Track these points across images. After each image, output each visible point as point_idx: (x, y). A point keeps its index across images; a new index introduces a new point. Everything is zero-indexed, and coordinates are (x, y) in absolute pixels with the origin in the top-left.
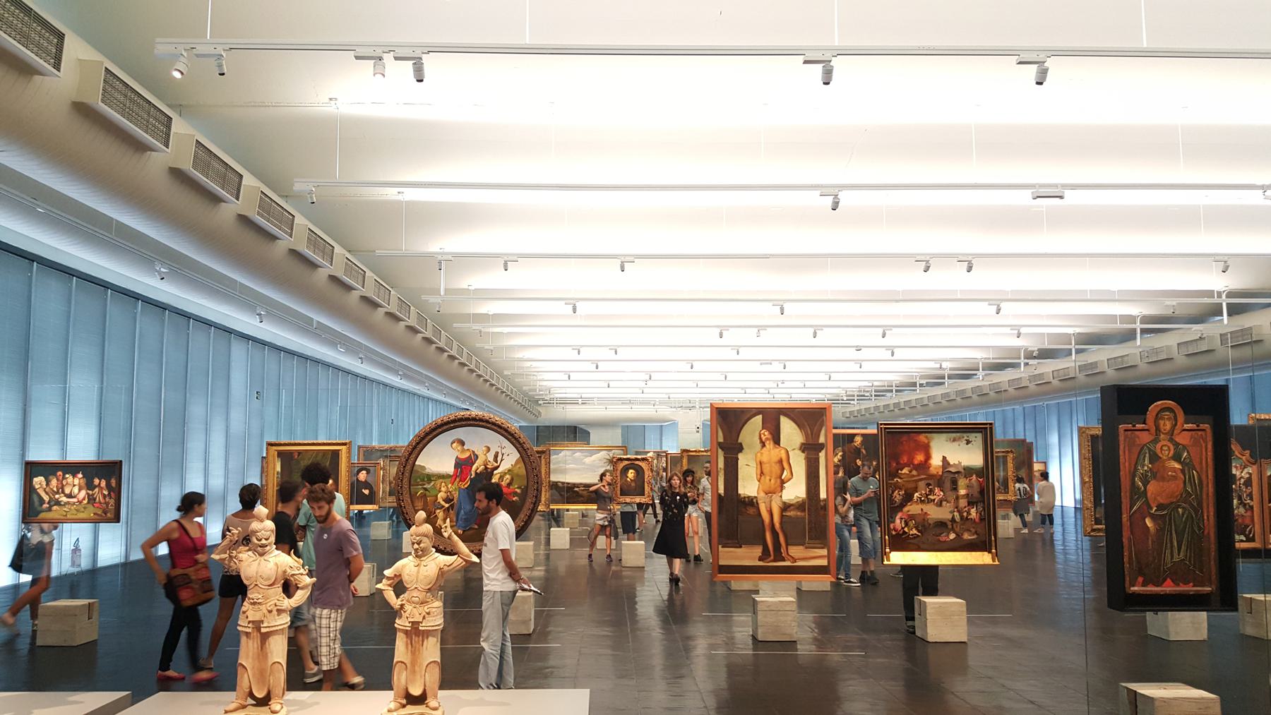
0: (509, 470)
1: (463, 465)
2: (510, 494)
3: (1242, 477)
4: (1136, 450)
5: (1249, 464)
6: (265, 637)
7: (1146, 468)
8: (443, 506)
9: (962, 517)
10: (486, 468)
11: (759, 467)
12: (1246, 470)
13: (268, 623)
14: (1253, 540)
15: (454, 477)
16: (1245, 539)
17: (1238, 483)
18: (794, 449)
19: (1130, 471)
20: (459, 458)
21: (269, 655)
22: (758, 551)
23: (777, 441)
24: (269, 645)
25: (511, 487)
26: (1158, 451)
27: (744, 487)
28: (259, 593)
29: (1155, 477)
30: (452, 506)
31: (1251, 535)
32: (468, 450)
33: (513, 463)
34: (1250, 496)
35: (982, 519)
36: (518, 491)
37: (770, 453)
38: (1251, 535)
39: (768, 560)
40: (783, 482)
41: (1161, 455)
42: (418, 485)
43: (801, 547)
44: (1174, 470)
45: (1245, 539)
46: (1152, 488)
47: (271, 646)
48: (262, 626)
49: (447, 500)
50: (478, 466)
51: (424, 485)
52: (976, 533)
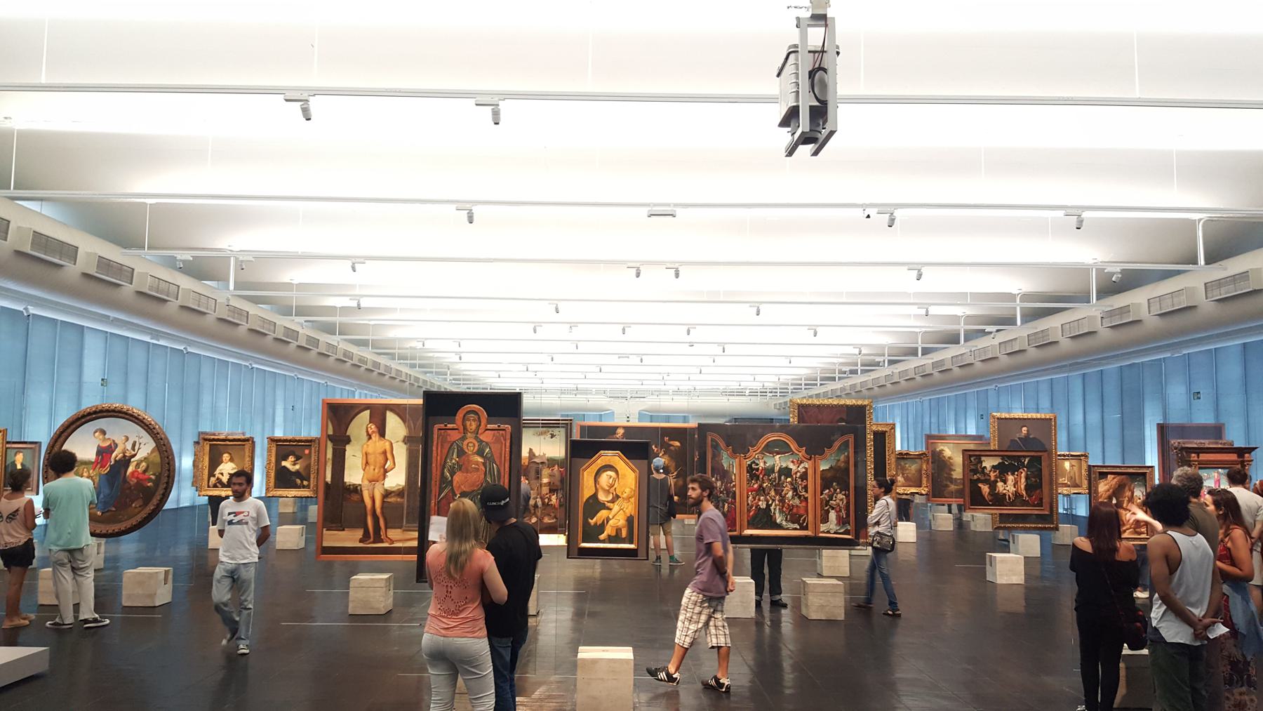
0: (145, 458)
1: (104, 453)
2: (145, 480)
3: (798, 471)
4: (447, 446)
5: (805, 459)
7: (454, 461)
9: (543, 503)
10: (124, 456)
11: (365, 457)
12: (802, 465)
14: (806, 528)
15: (95, 465)
16: (798, 527)
17: (794, 476)
18: (398, 442)
19: (440, 464)
20: (102, 447)
22: (359, 533)
23: (382, 434)
25: (147, 474)
26: (465, 447)
27: (350, 475)
29: (460, 468)
31: (805, 524)
32: (109, 439)
33: (149, 452)
34: (806, 488)
35: (560, 506)
36: (153, 477)
37: (377, 445)
38: (805, 524)
39: (368, 542)
40: (386, 471)
41: (467, 451)
43: (399, 530)
44: (477, 463)
45: (798, 527)
46: (458, 478)
50: (117, 454)
52: (555, 517)
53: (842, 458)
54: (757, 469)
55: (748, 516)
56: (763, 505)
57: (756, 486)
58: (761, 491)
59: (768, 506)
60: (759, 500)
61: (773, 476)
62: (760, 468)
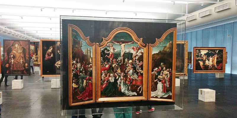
3: (137, 55)
12: (140, 51)
14: (141, 95)
16: (136, 94)
17: (134, 59)
31: (140, 92)
34: (142, 67)
38: (140, 92)
45: (136, 94)
53: (168, 45)
54: (109, 54)
55: (101, 88)
56: (112, 80)
57: (107, 66)
58: (111, 69)
59: (116, 80)
60: (110, 76)
61: (119, 59)
62: (111, 53)
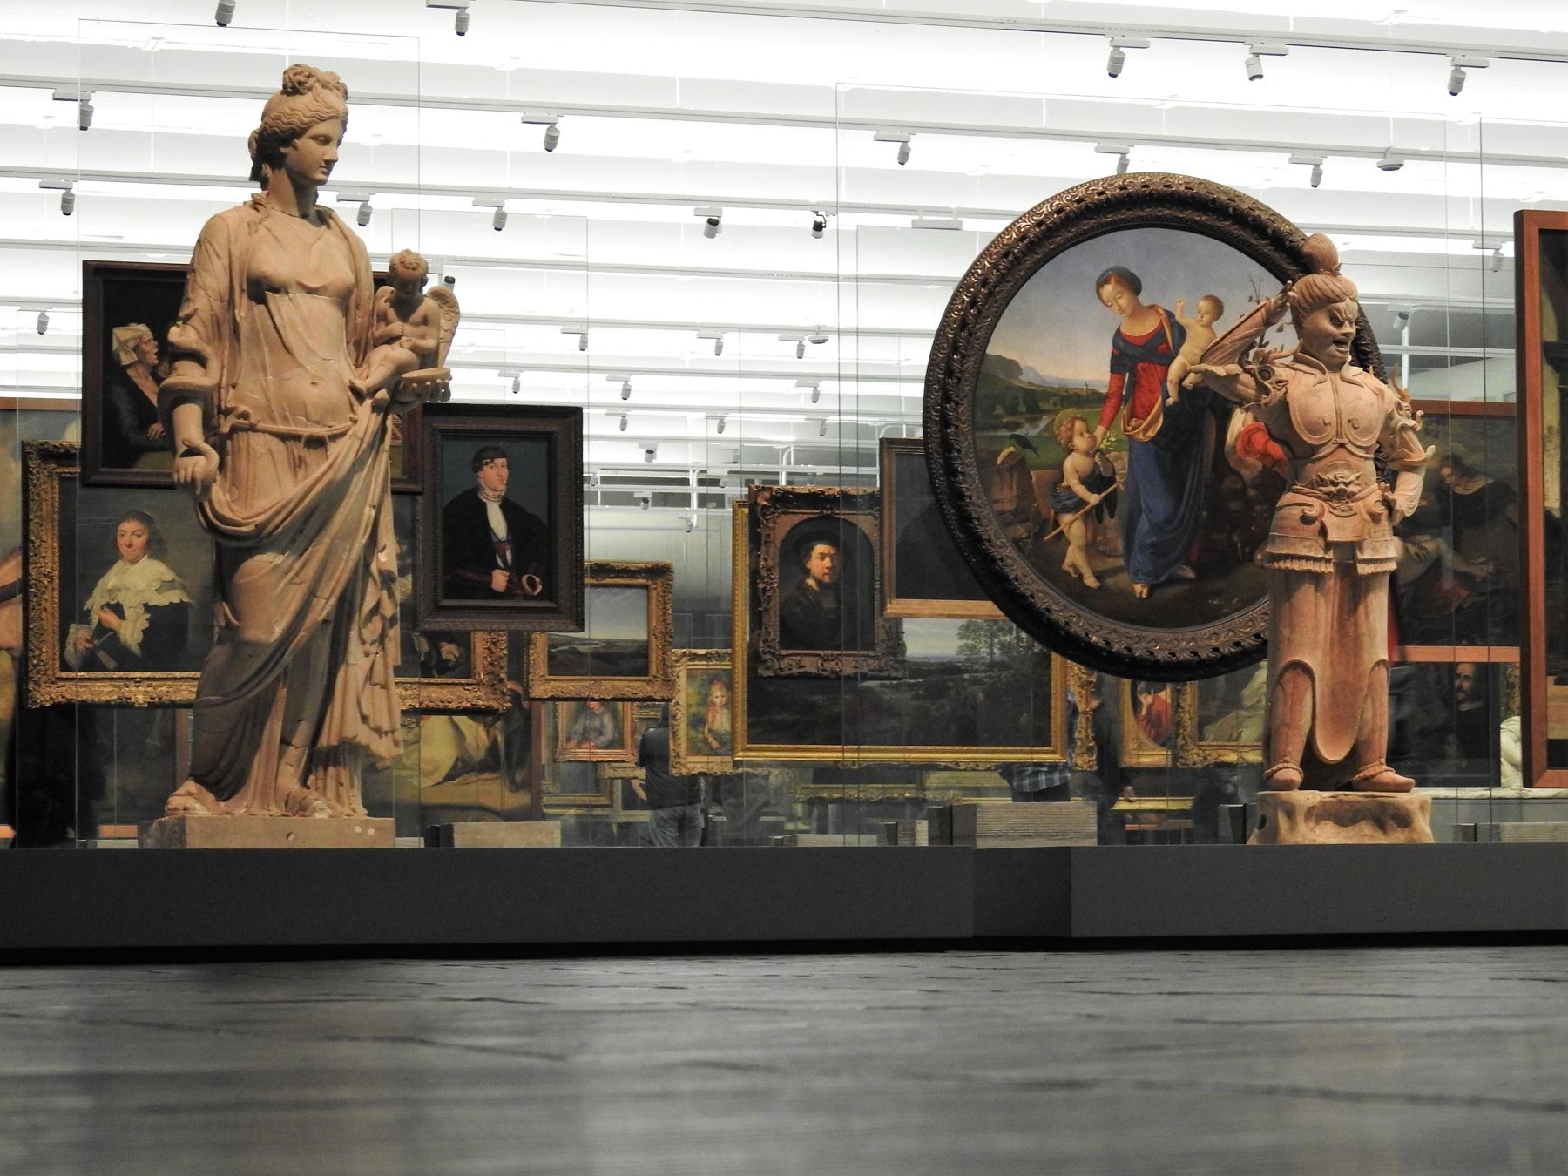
6: (1355, 588)
8: (1082, 503)
13: (1374, 549)
21: (1366, 640)
24: (1367, 614)
28: (1348, 467)
30: (1110, 503)
32: (1152, 307)
42: (995, 428)
47: (1372, 616)
48: (1360, 556)
49: (1095, 481)
51: (1017, 426)
